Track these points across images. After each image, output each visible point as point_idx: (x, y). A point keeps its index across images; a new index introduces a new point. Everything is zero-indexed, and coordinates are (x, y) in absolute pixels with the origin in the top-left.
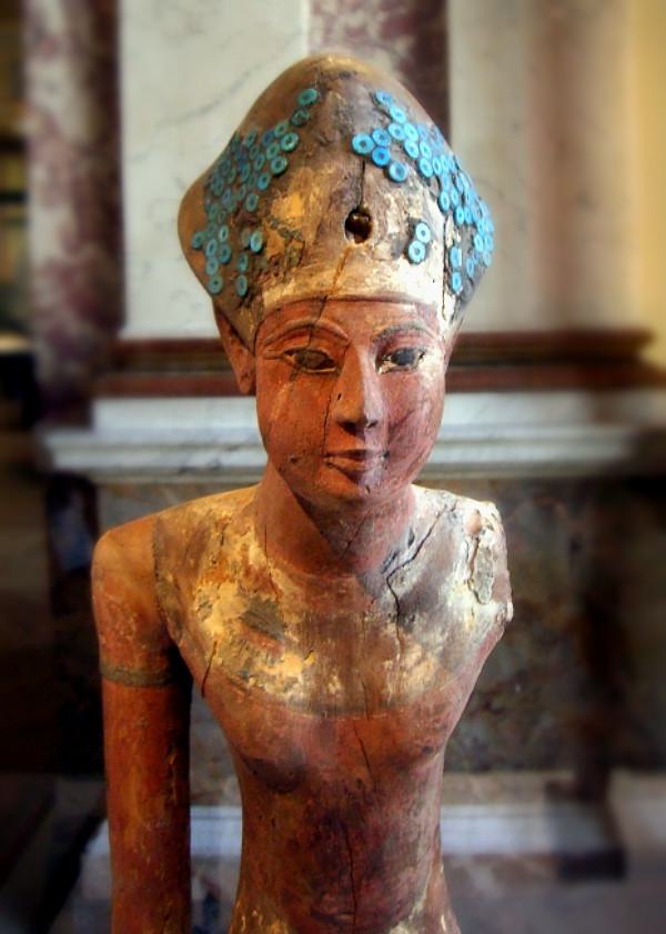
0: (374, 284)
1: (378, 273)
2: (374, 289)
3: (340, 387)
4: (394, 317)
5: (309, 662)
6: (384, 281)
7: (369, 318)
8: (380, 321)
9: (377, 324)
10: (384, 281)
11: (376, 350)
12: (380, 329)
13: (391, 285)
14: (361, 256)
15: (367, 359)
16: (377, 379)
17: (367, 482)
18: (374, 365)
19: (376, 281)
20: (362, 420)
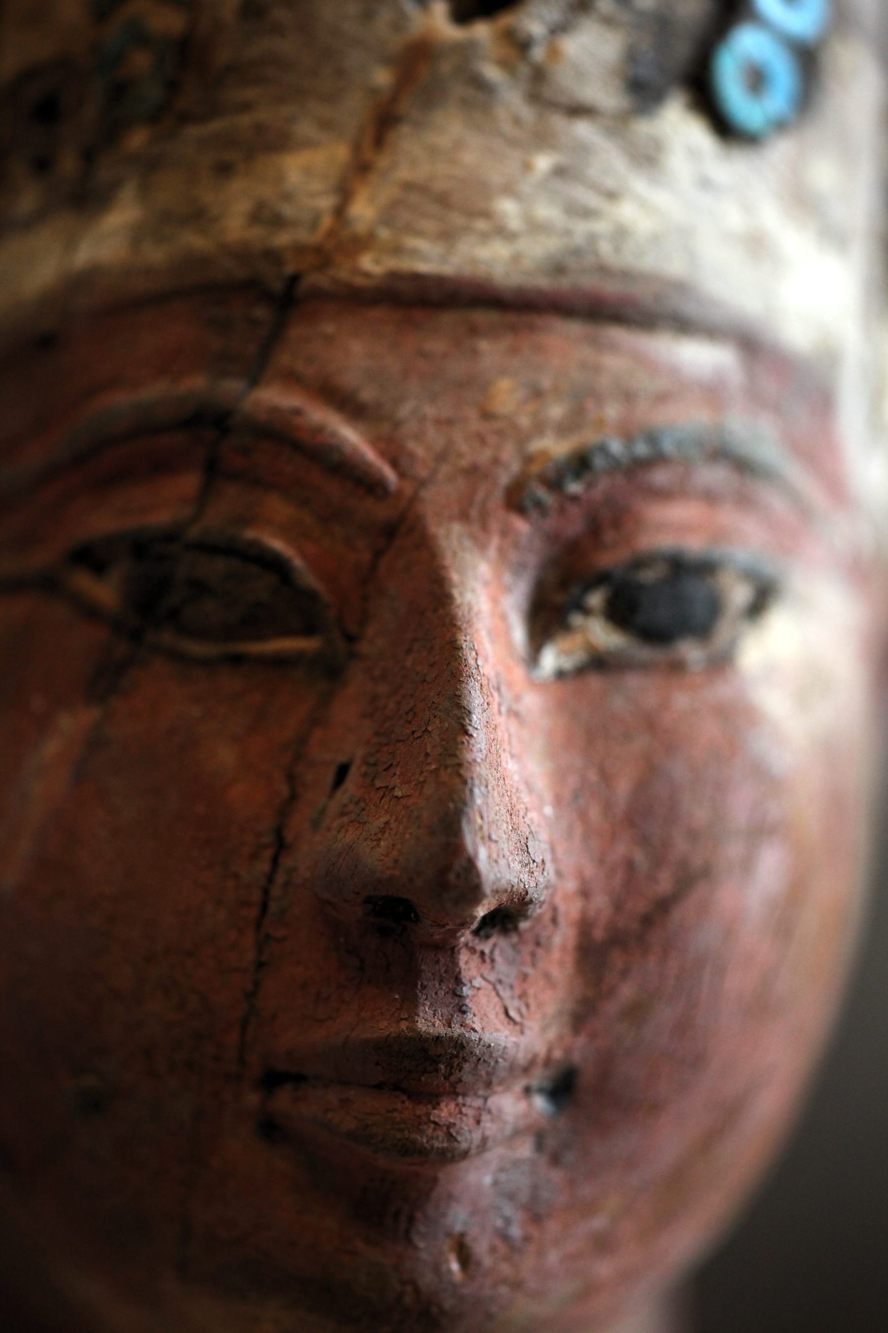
0: (536, 227)
1: (560, 172)
2: (537, 250)
3: (347, 731)
4: (628, 397)
5: (492, 552)
6: (588, 213)
7: (507, 395)
8: (556, 411)
9: (539, 428)
10: (588, 213)
11: (532, 560)
12: (556, 447)
13: (621, 233)
14: (479, 83)
15: (489, 601)
16: (532, 702)
17: (458, 1217)
18: (519, 634)
19: (547, 211)
20: (455, 876)
